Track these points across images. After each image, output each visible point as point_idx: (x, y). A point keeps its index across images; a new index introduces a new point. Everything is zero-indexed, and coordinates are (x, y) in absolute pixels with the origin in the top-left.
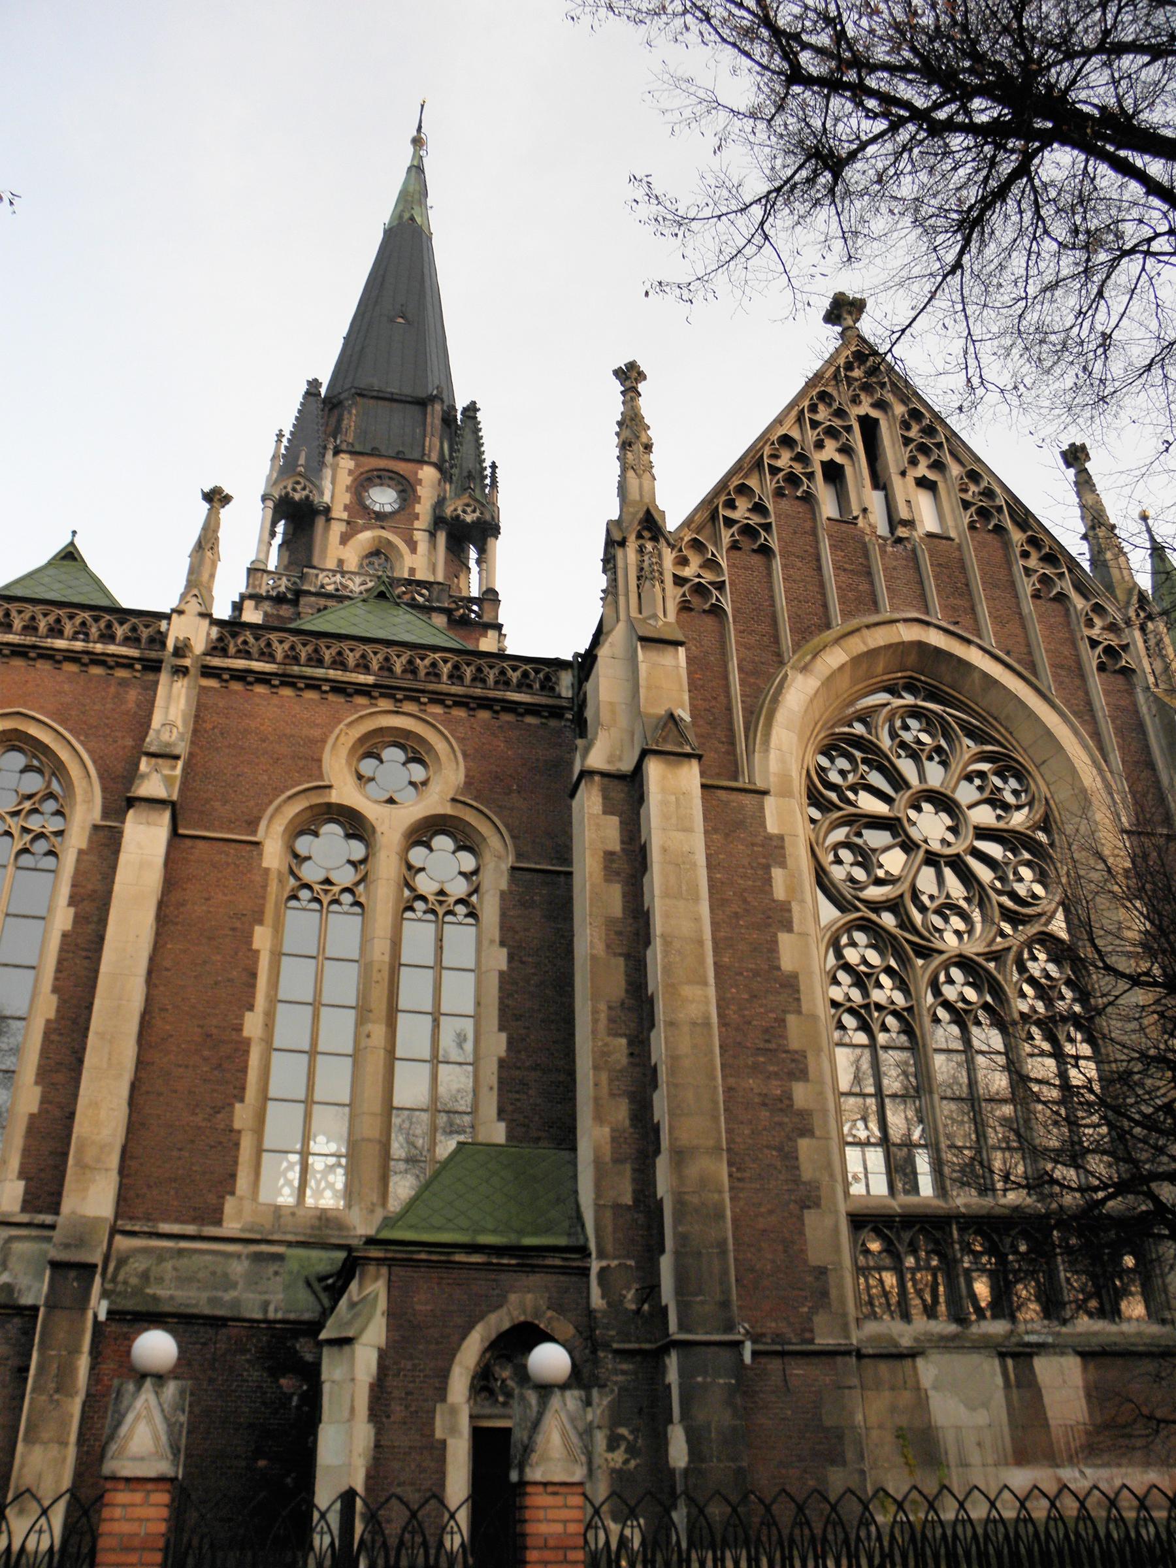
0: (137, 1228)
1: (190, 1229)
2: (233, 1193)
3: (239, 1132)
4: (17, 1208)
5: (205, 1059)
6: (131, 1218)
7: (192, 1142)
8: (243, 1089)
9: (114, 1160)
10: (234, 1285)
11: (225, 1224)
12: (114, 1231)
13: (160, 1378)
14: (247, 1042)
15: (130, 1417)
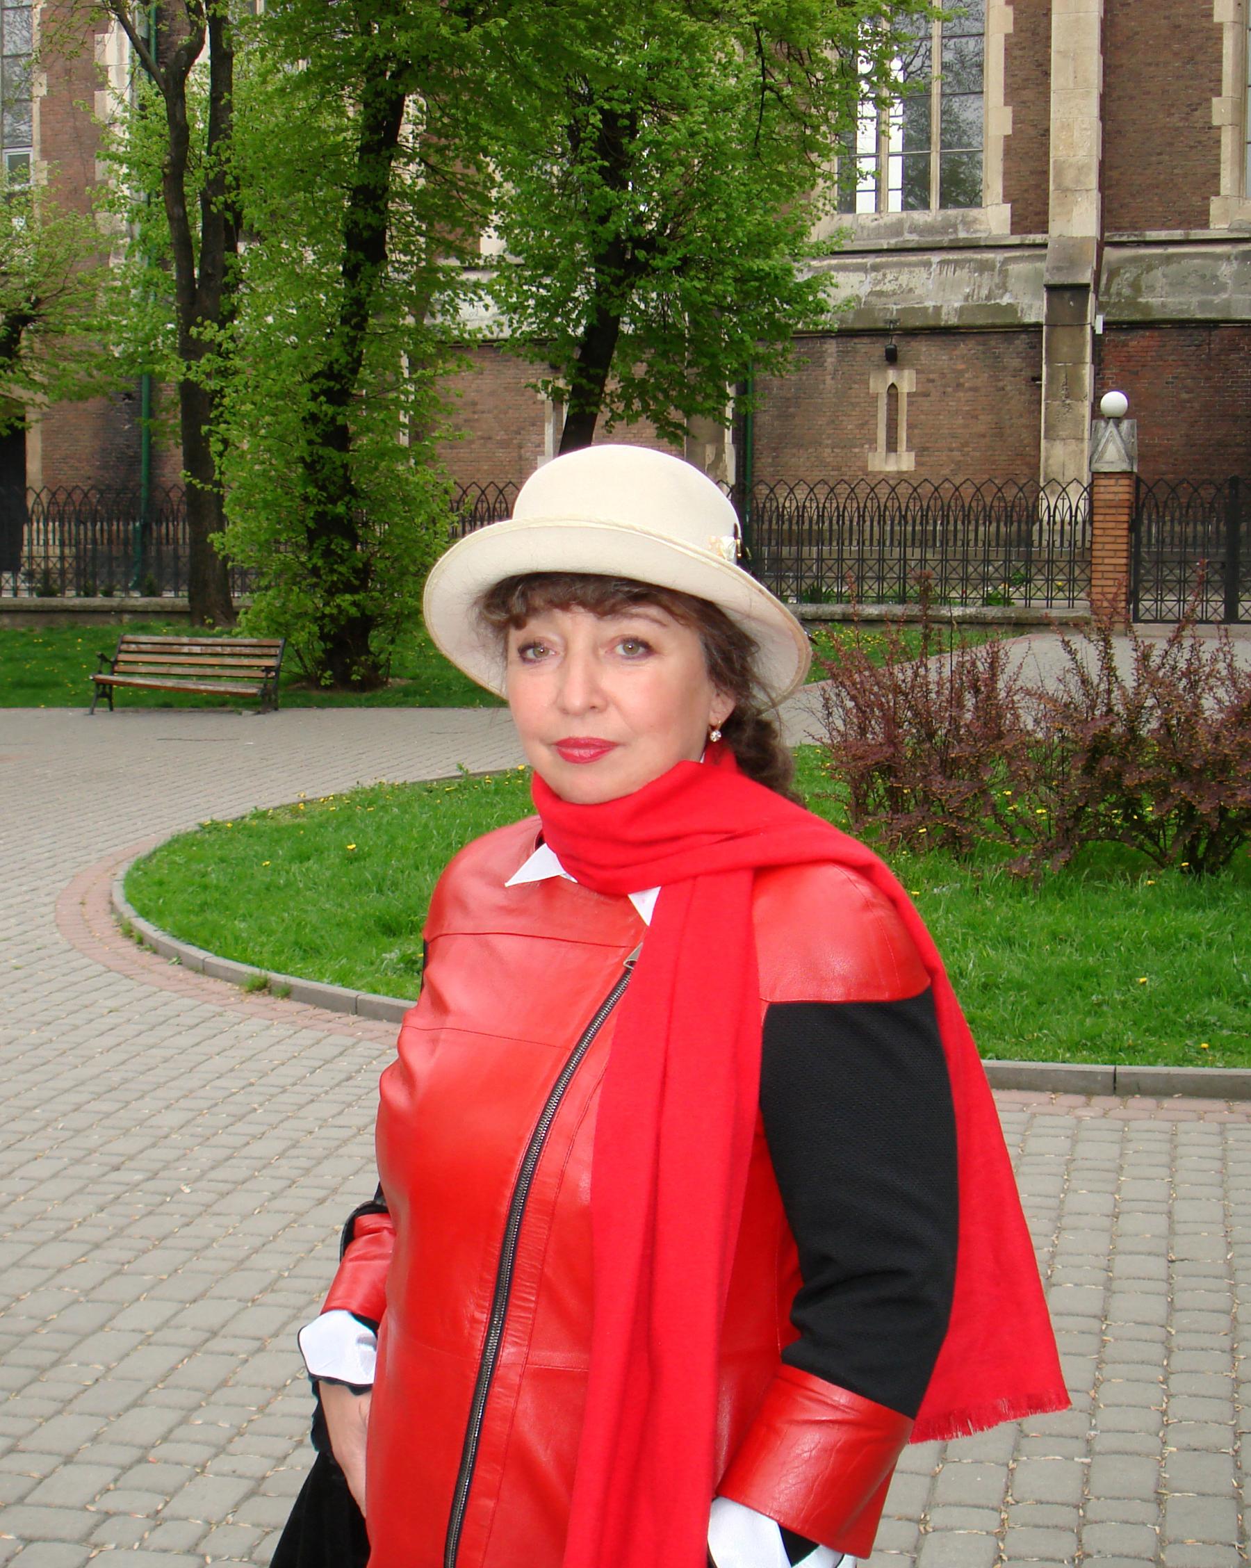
0: (1124, 239)
1: (1177, 234)
2: (1217, 194)
3: (1219, 128)
4: (1007, 230)
5: (1176, 54)
6: (1118, 229)
7: (1171, 144)
8: (1220, 81)
9: (1093, 180)
10: (1222, 288)
11: (1212, 226)
12: (1102, 244)
13: (1118, 420)
14: (1219, 28)
15: (1103, 441)
